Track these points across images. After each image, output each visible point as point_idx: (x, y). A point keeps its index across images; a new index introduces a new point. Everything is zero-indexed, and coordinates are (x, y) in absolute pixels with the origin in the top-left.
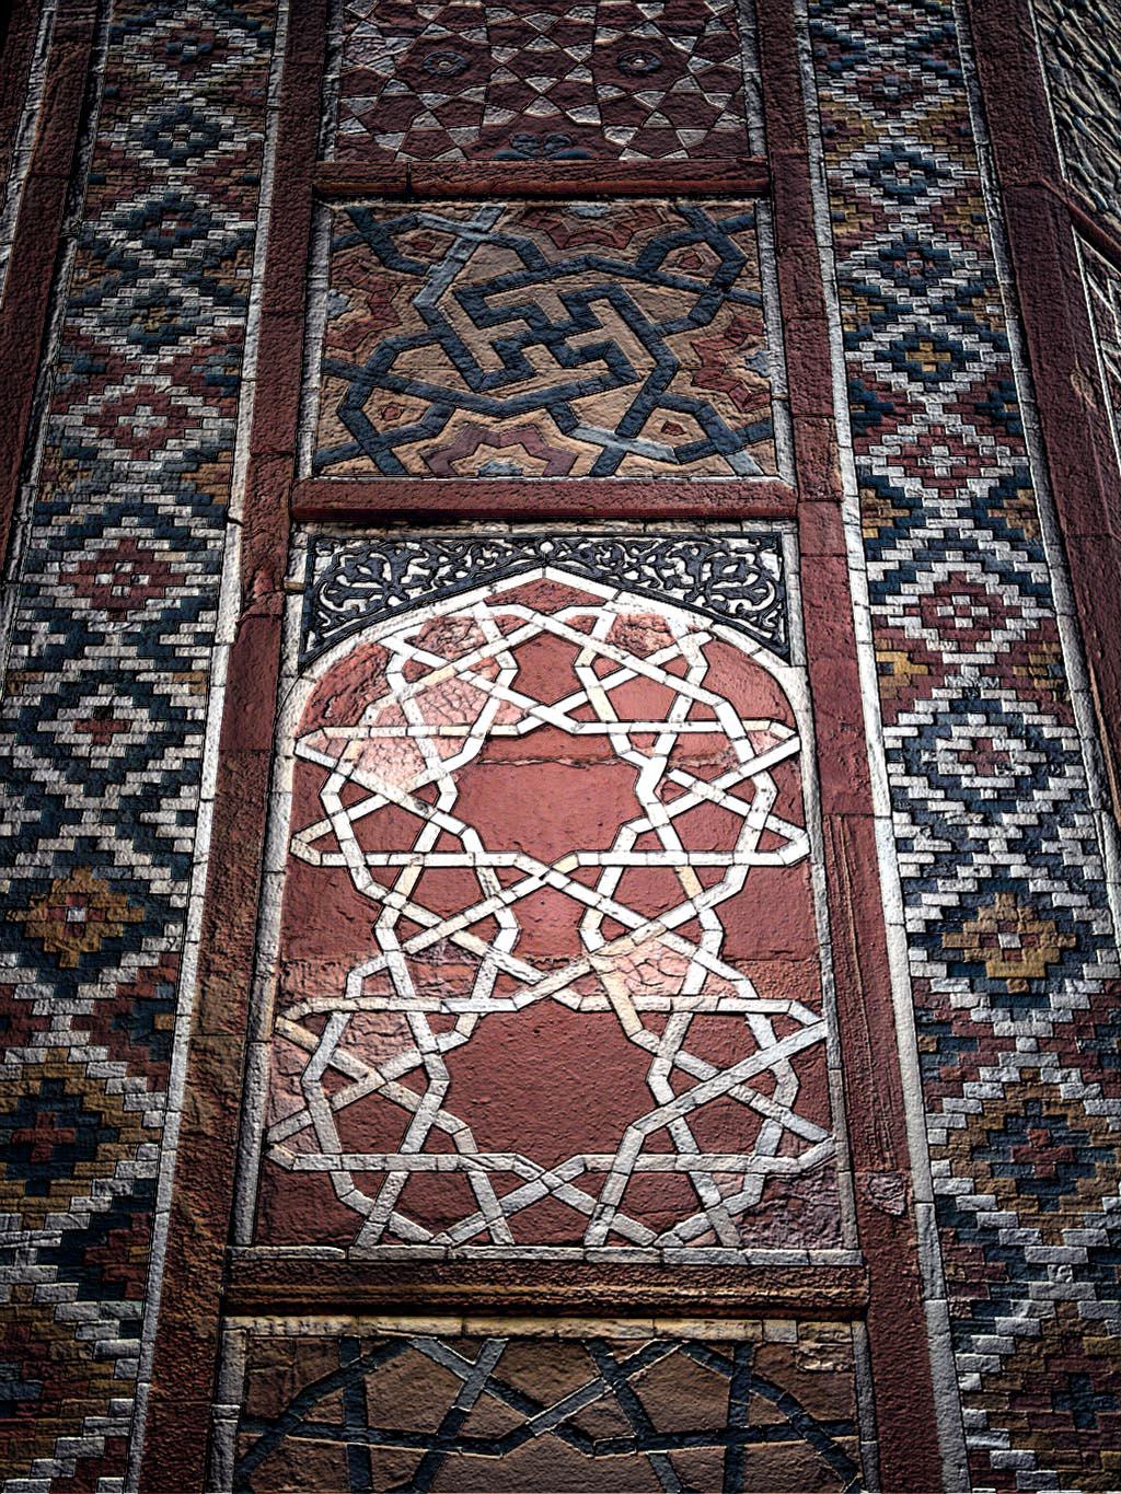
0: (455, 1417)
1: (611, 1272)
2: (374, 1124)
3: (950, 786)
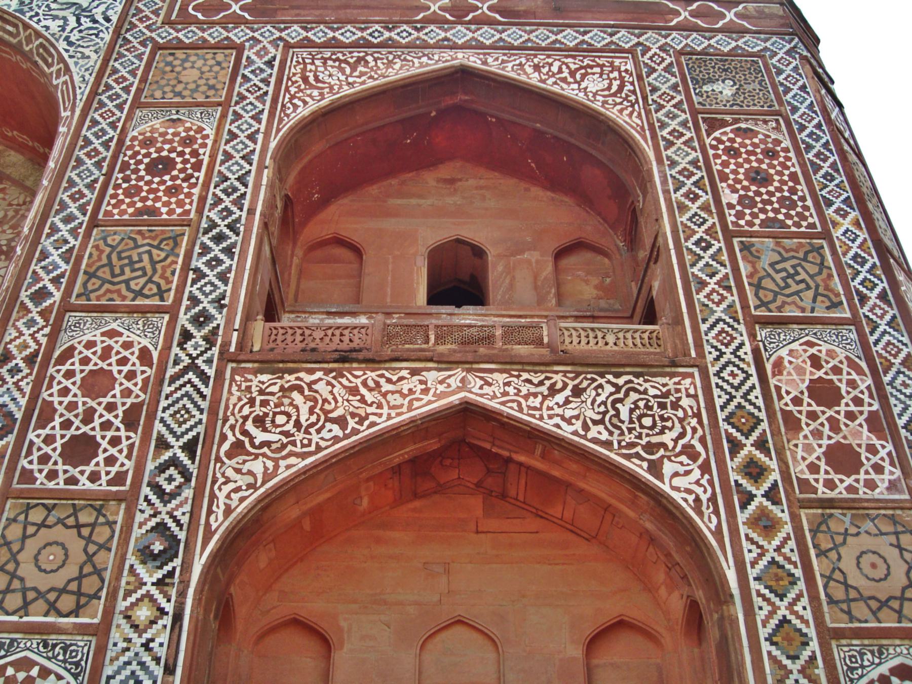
0: (846, 530)
2: (814, 468)
3: (900, 391)
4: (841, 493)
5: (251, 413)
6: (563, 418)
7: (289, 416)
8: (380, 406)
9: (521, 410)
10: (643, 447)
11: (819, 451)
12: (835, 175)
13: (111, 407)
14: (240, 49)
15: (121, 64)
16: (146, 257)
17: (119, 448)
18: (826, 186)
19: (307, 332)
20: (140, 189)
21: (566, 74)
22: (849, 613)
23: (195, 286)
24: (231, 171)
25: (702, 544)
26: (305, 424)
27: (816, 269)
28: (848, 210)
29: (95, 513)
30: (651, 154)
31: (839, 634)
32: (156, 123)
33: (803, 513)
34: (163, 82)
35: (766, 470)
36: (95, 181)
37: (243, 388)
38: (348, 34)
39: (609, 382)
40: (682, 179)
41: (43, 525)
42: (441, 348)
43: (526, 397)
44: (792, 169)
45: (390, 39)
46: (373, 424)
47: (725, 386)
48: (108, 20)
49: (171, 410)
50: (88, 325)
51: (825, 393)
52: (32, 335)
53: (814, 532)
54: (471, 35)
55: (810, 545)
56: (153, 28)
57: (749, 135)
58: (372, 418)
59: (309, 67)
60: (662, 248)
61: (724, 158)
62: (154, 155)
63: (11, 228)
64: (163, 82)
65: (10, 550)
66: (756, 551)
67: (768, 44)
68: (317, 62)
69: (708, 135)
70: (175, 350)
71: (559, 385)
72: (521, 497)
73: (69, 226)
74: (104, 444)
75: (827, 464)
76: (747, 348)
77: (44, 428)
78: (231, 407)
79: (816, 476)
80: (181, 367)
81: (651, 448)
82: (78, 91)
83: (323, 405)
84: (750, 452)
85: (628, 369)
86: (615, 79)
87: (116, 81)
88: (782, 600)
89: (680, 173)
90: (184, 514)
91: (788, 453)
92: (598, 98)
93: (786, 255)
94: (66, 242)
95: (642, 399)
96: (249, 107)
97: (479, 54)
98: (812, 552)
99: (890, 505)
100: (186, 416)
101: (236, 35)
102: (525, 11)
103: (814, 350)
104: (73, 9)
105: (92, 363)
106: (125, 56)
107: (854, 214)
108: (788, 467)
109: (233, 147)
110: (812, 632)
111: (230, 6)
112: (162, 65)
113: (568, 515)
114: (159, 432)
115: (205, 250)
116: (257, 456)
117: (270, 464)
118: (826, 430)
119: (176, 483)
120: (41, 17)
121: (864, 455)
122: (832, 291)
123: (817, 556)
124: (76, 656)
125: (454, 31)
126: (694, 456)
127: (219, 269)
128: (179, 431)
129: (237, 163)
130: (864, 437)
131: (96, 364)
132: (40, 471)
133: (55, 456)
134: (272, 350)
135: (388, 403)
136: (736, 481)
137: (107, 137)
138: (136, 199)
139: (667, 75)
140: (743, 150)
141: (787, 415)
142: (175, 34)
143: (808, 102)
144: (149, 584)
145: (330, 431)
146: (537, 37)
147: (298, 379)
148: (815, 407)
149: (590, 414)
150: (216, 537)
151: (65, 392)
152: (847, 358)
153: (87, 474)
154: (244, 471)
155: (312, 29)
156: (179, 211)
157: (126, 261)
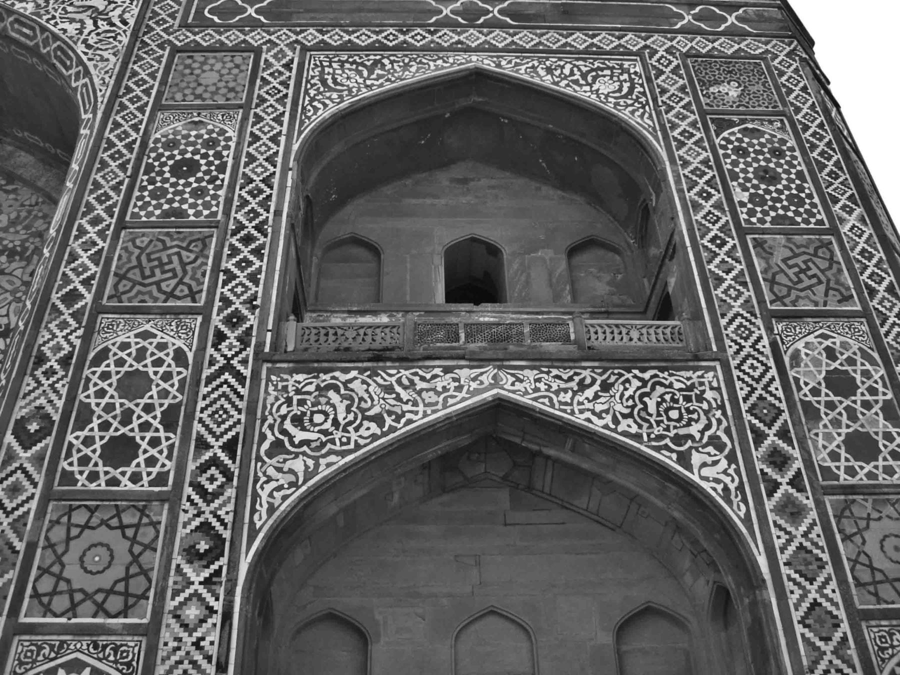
1: (887, 486)
5: (289, 412)
6: (593, 412)
7: (326, 414)
8: (415, 404)
9: (552, 405)
10: (672, 439)
11: (839, 440)
12: (840, 173)
13: (148, 409)
14: (258, 52)
15: (140, 67)
16: (175, 259)
17: (159, 448)
18: (832, 184)
19: (340, 332)
20: (166, 191)
21: (577, 76)
22: (876, 594)
23: (226, 288)
24: (256, 173)
25: (733, 533)
26: (343, 423)
27: (826, 264)
28: (854, 206)
29: (138, 514)
30: (664, 154)
31: (868, 615)
32: (179, 126)
33: (827, 499)
34: (184, 85)
35: (789, 459)
36: (121, 183)
37: (280, 387)
38: (363, 37)
39: (635, 377)
40: (694, 178)
41: (86, 526)
42: (472, 346)
43: (557, 392)
44: (799, 168)
45: (405, 42)
46: (410, 422)
47: (747, 379)
48: (125, 23)
49: (210, 411)
50: (121, 327)
51: (841, 383)
52: (65, 337)
53: (839, 518)
54: (483, 38)
56: (168, 31)
57: (757, 134)
58: (409, 416)
59: (327, 70)
60: (678, 247)
61: (733, 157)
62: (178, 157)
63: (24, 228)
64: (184, 85)
65: (55, 552)
66: (784, 537)
67: (769, 47)
68: (335, 65)
69: (717, 136)
70: (210, 351)
71: (588, 381)
72: (547, 490)
73: (97, 228)
74: (144, 445)
75: (846, 452)
76: (765, 341)
77: (82, 429)
78: (269, 407)
79: (837, 464)
80: (216, 367)
81: (679, 440)
82: (99, 94)
83: (359, 403)
84: (773, 441)
85: (653, 364)
86: (625, 81)
87: (136, 83)
88: (811, 584)
89: (692, 172)
90: (227, 513)
92: (610, 99)
93: (797, 251)
94: (94, 244)
95: (668, 393)
96: (270, 110)
97: (492, 57)
98: (838, 537)
100: (224, 416)
101: (252, 38)
102: (534, 15)
103: (828, 343)
104: (89, 13)
105: (127, 364)
106: (144, 59)
107: (859, 211)
108: (810, 455)
109: (256, 149)
110: (842, 614)
111: (246, 10)
112: (181, 68)
113: (593, 506)
114: (198, 433)
115: (235, 251)
116: (297, 455)
117: (310, 463)
118: (844, 419)
119: (218, 483)
120: (59, 20)
121: (881, 442)
122: (842, 285)
123: (843, 540)
124: (127, 657)
125: (467, 34)
126: (720, 447)
127: (249, 270)
128: (218, 431)
129: (261, 165)
130: (881, 426)
131: (131, 366)
132: (81, 473)
133: (95, 457)
134: (306, 349)
135: (423, 400)
136: (762, 470)
137: (130, 139)
138: (163, 201)
139: (674, 77)
140: (751, 150)
141: (807, 405)
142: (192, 37)
143: (810, 102)
144: (197, 583)
145: (368, 429)
146: (547, 40)
147: (333, 378)
148: (832, 398)
149: (619, 408)
150: (261, 535)
151: (101, 393)
152: (860, 349)
153: (128, 475)
154: (285, 469)
155: (328, 32)
156: (206, 212)
157: (156, 263)
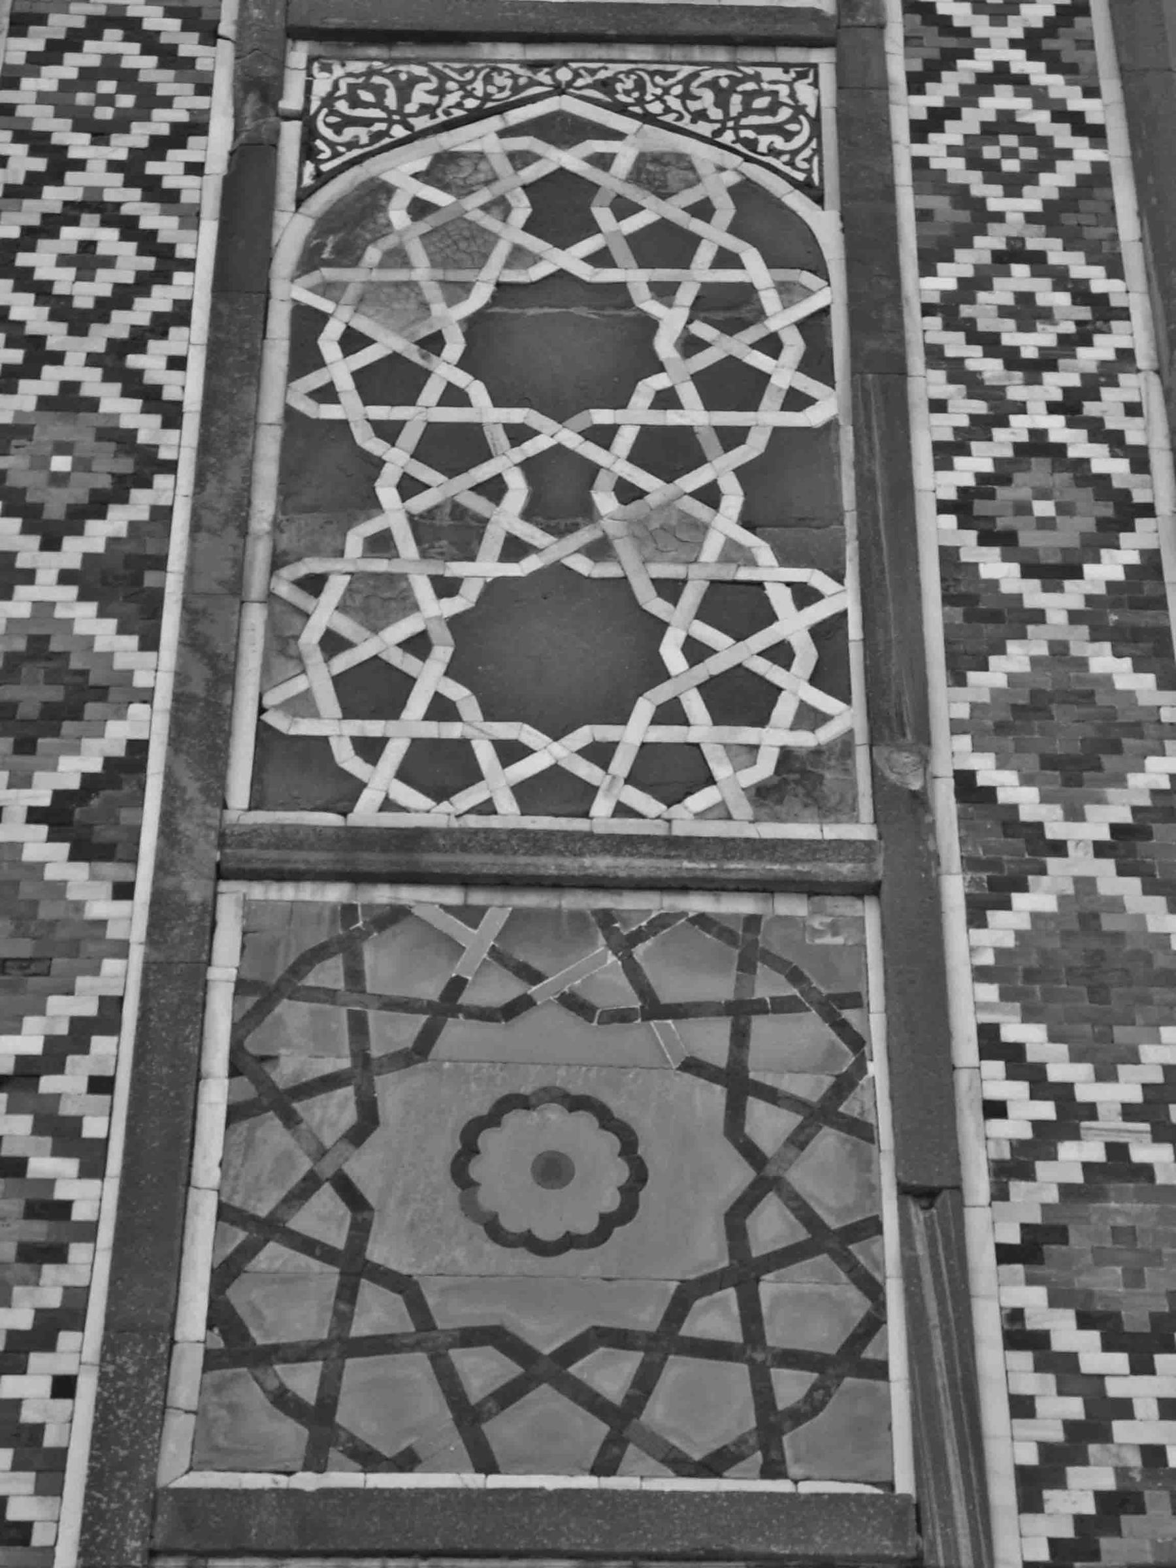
0: (457, 985)
2: (374, 691)
3: (991, 344)
4: (487, 808)
11: (433, 610)
55: (217, 1057)
76: (216, 147)
91: (255, 618)
99: (738, 867)
152: (744, 192)
